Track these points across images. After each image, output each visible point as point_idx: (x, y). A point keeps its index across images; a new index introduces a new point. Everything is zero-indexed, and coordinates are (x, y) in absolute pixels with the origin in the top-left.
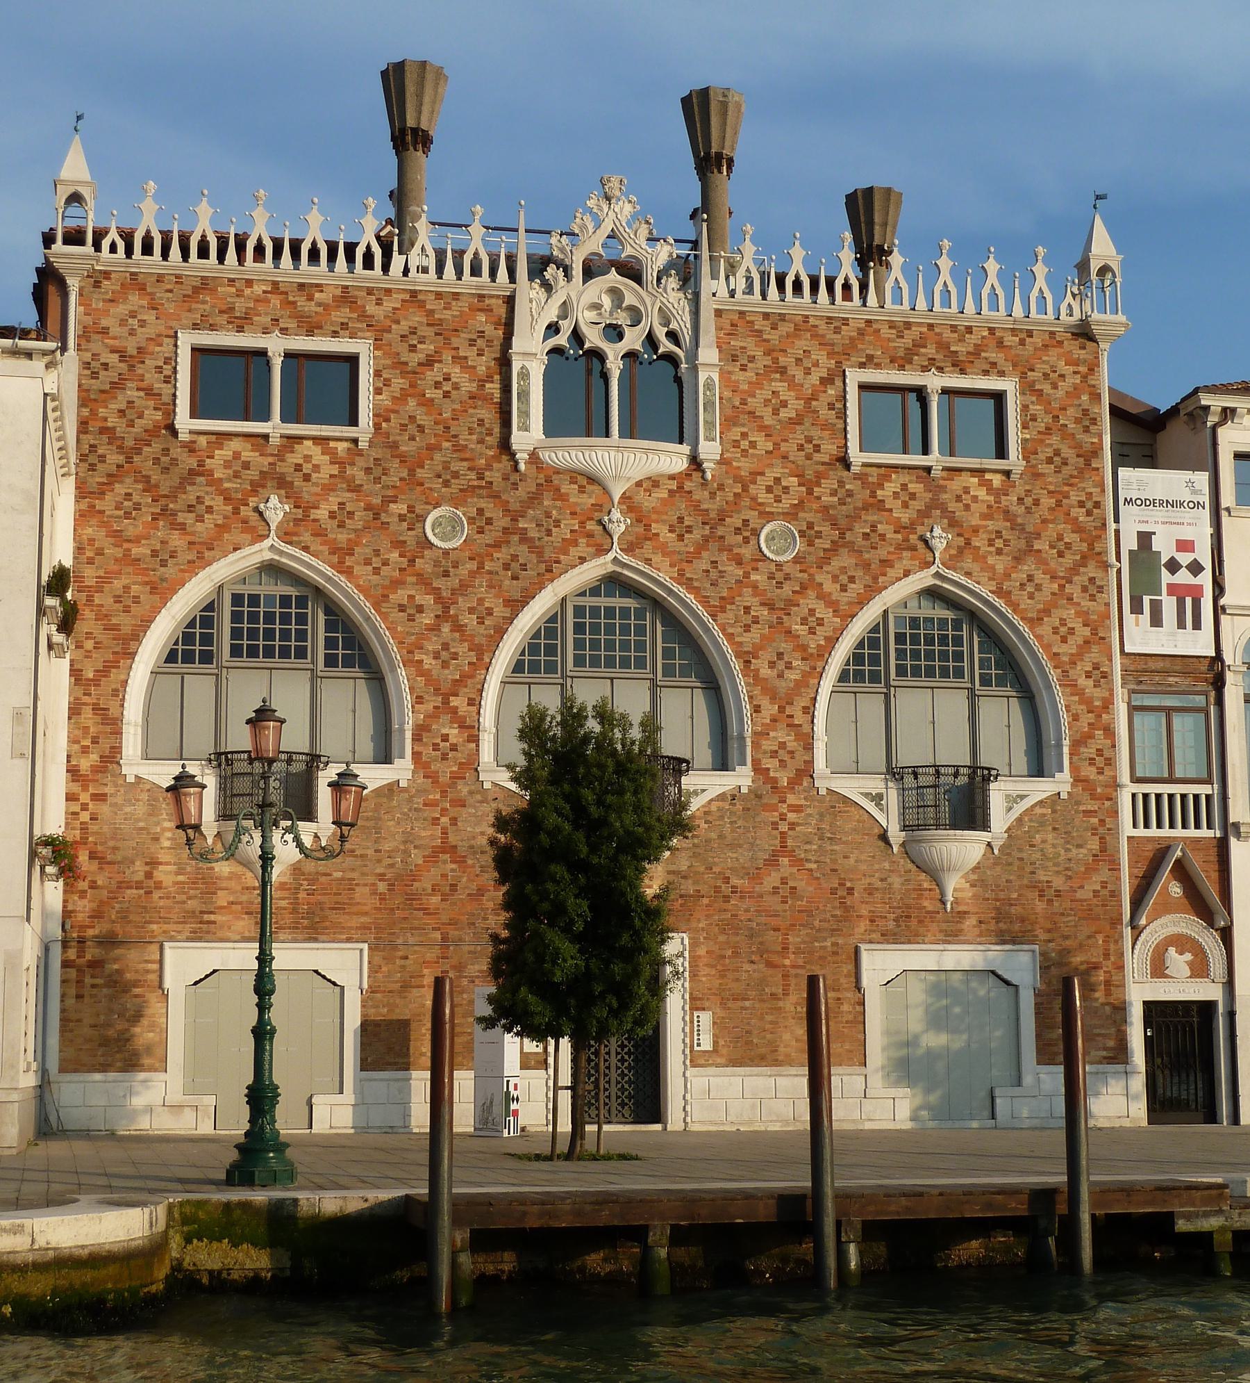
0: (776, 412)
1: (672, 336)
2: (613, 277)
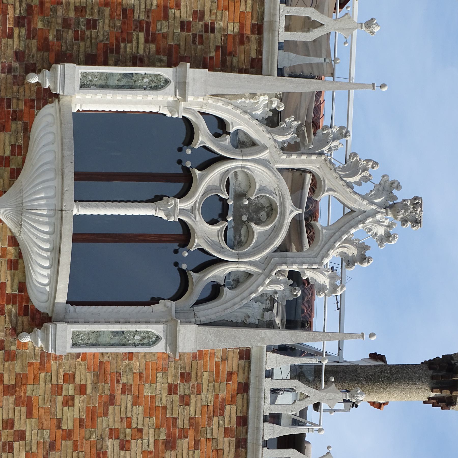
0: (114, 434)
1: (215, 291)
2: (291, 212)
